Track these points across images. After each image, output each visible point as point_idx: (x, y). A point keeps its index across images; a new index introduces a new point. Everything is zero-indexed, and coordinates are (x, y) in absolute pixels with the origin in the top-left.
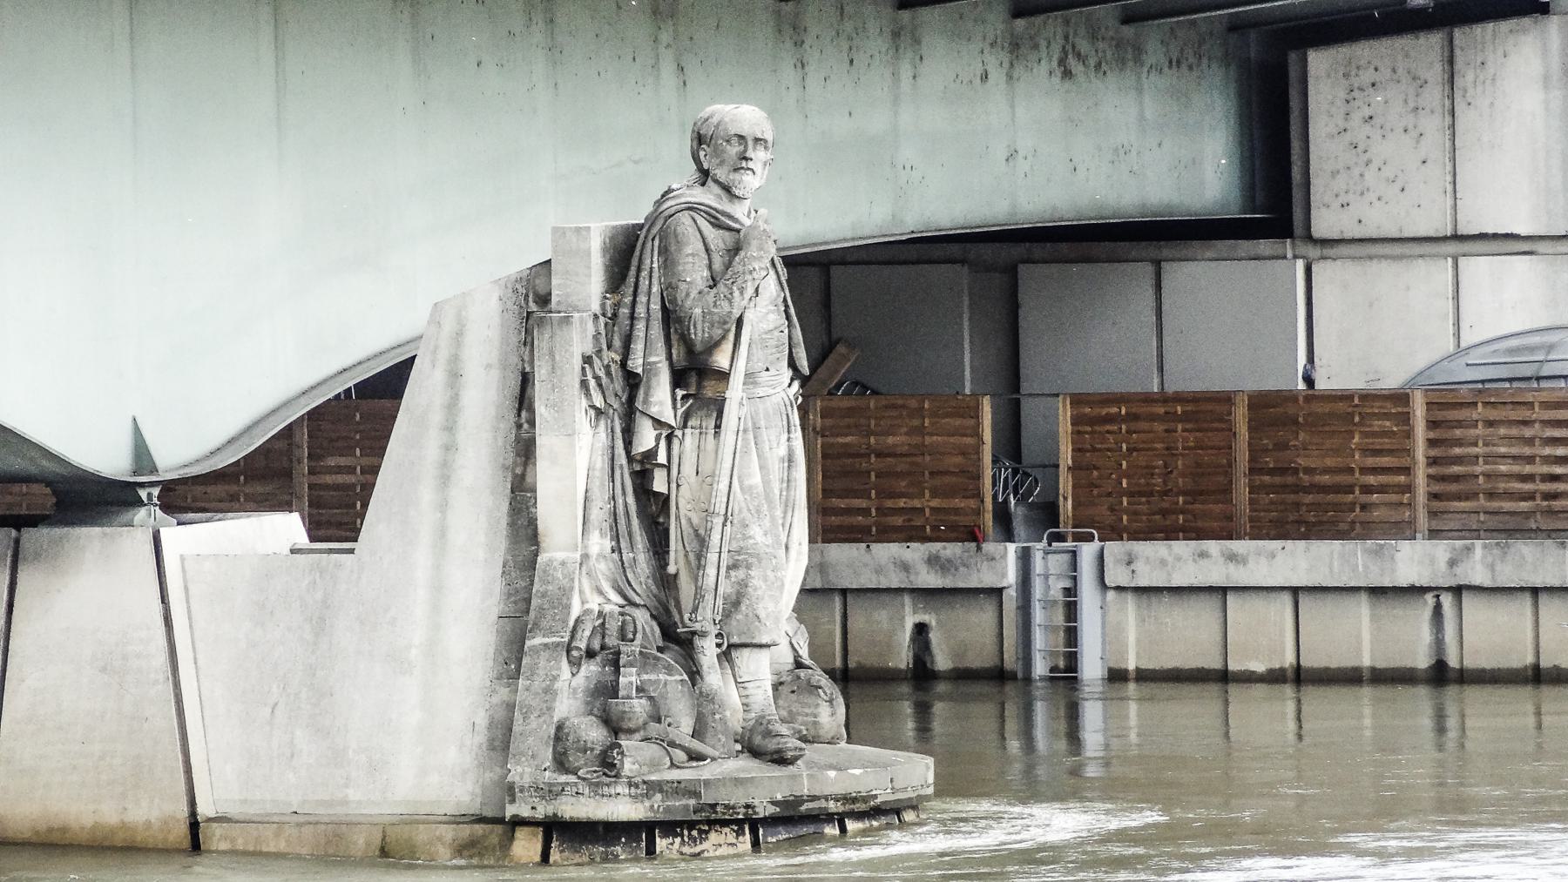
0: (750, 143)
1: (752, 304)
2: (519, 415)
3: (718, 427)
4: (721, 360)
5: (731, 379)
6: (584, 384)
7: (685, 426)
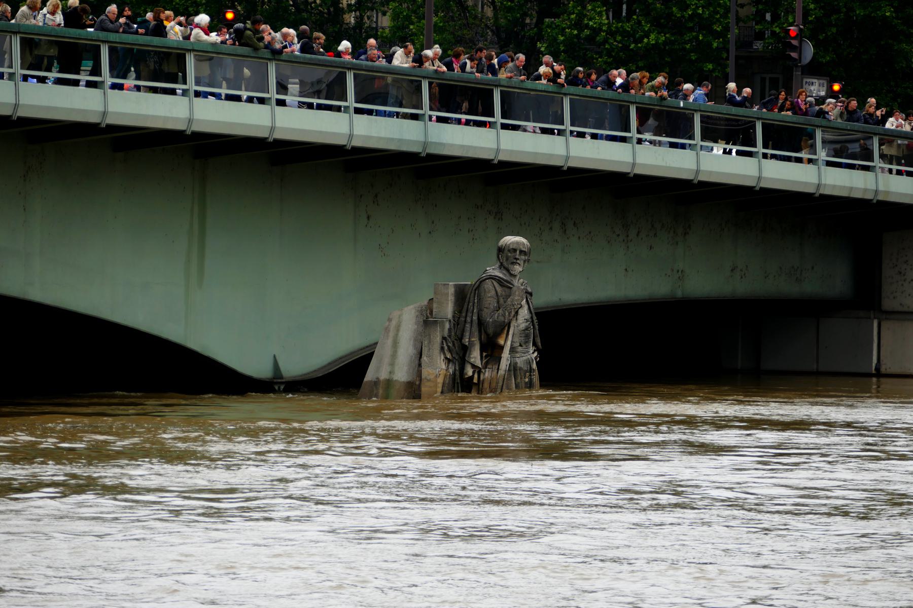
0: (518, 252)
1: (515, 319)
4: (501, 342)
6: (442, 349)
7: (485, 367)
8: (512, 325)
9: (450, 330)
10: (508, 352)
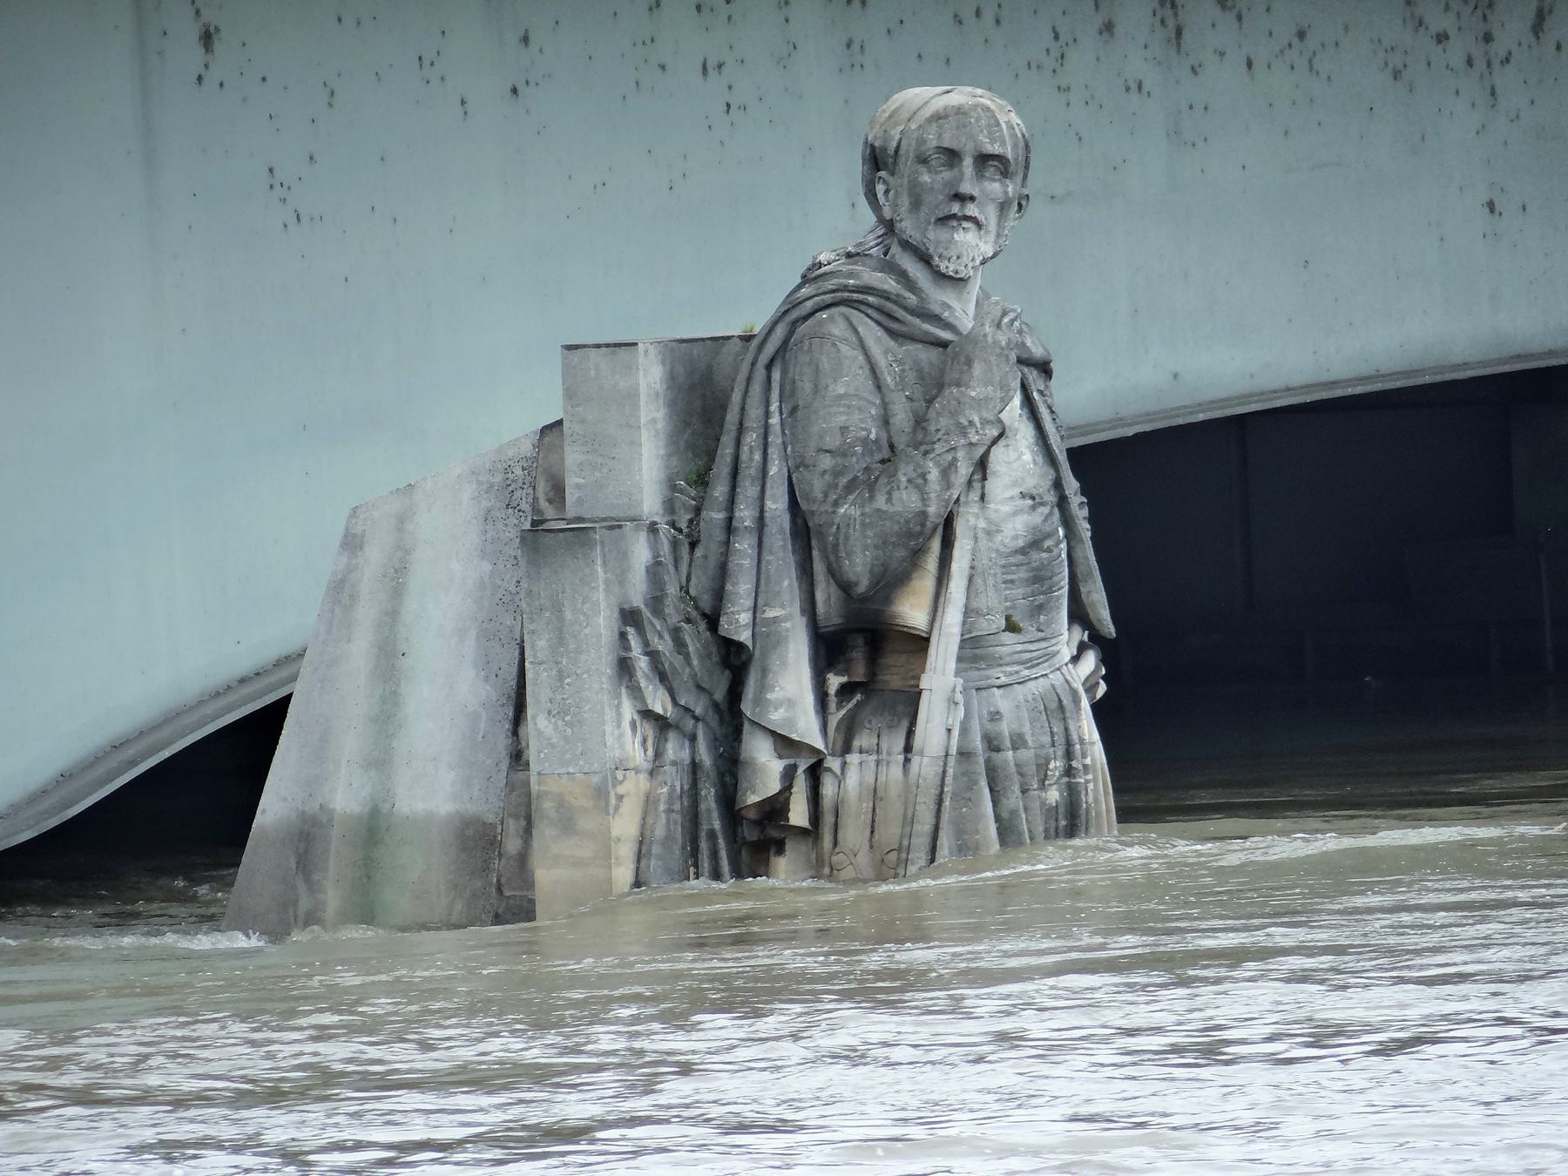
0: (968, 163)
1: (974, 496)
4: (912, 612)
6: (624, 667)
7: (847, 749)
8: (960, 528)
9: (655, 571)
10: (952, 665)
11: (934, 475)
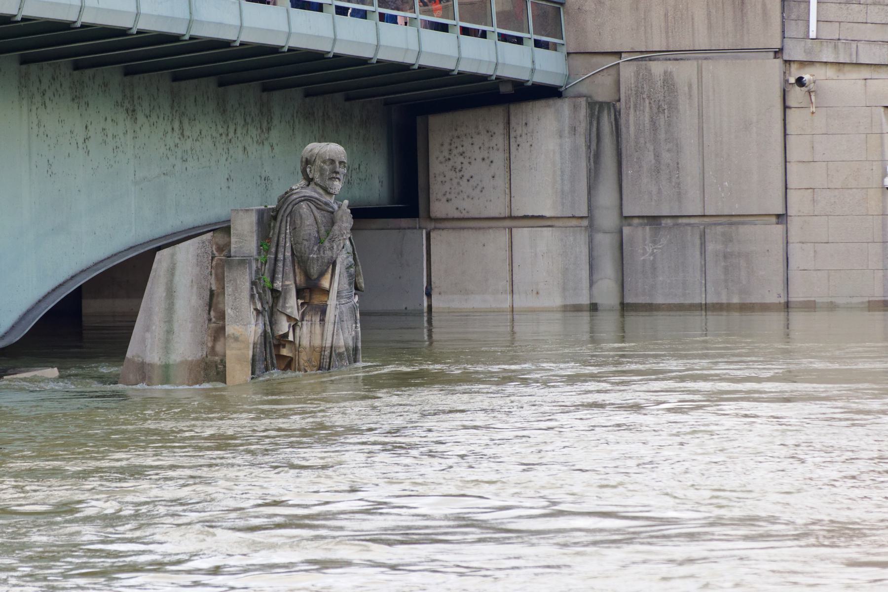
0: (337, 163)
2: (209, 314)
3: (322, 320)
4: (325, 283)
5: (331, 294)
6: (252, 296)
7: (302, 320)
11: (335, 247)
